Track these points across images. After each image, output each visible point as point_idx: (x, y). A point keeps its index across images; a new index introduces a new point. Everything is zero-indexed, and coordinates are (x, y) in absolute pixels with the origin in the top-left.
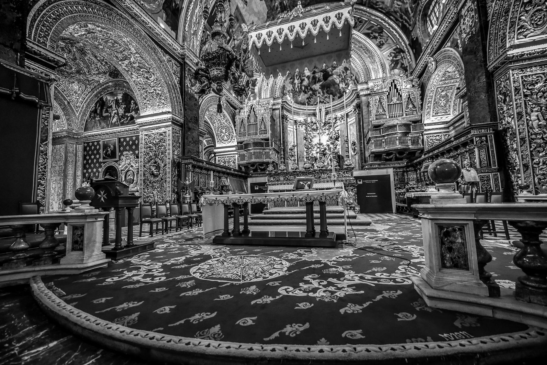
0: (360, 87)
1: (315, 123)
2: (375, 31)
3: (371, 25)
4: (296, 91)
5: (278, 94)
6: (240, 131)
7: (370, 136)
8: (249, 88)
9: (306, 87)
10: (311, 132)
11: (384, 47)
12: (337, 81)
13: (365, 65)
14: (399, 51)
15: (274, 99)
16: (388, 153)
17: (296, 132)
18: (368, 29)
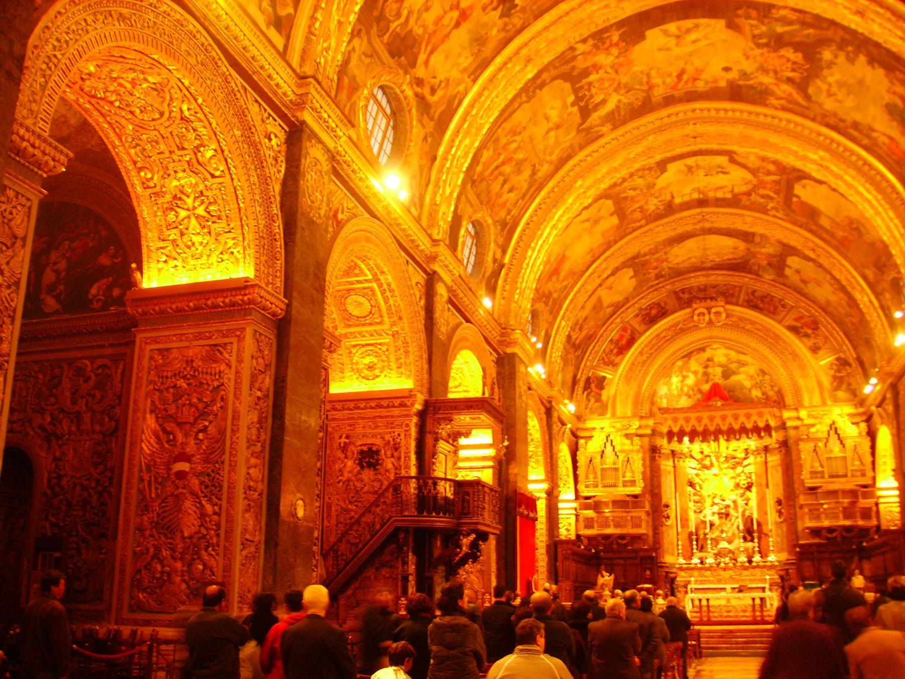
0: (786, 414)
1: (709, 456)
2: (806, 325)
3: (800, 315)
4: (673, 395)
5: (646, 409)
6: (587, 477)
7: (802, 502)
8: (592, 391)
9: (690, 388)
10: (700, 472)
11: (821, 352)
12: (748, 384)
13: (792, 378)
14: (843, 363)
15: (641, 418)
16: (830, 530)
17: (675, 471)
18: (796, 320)
